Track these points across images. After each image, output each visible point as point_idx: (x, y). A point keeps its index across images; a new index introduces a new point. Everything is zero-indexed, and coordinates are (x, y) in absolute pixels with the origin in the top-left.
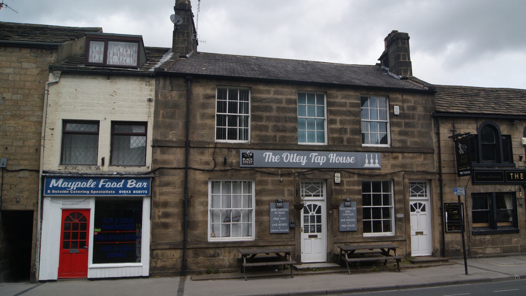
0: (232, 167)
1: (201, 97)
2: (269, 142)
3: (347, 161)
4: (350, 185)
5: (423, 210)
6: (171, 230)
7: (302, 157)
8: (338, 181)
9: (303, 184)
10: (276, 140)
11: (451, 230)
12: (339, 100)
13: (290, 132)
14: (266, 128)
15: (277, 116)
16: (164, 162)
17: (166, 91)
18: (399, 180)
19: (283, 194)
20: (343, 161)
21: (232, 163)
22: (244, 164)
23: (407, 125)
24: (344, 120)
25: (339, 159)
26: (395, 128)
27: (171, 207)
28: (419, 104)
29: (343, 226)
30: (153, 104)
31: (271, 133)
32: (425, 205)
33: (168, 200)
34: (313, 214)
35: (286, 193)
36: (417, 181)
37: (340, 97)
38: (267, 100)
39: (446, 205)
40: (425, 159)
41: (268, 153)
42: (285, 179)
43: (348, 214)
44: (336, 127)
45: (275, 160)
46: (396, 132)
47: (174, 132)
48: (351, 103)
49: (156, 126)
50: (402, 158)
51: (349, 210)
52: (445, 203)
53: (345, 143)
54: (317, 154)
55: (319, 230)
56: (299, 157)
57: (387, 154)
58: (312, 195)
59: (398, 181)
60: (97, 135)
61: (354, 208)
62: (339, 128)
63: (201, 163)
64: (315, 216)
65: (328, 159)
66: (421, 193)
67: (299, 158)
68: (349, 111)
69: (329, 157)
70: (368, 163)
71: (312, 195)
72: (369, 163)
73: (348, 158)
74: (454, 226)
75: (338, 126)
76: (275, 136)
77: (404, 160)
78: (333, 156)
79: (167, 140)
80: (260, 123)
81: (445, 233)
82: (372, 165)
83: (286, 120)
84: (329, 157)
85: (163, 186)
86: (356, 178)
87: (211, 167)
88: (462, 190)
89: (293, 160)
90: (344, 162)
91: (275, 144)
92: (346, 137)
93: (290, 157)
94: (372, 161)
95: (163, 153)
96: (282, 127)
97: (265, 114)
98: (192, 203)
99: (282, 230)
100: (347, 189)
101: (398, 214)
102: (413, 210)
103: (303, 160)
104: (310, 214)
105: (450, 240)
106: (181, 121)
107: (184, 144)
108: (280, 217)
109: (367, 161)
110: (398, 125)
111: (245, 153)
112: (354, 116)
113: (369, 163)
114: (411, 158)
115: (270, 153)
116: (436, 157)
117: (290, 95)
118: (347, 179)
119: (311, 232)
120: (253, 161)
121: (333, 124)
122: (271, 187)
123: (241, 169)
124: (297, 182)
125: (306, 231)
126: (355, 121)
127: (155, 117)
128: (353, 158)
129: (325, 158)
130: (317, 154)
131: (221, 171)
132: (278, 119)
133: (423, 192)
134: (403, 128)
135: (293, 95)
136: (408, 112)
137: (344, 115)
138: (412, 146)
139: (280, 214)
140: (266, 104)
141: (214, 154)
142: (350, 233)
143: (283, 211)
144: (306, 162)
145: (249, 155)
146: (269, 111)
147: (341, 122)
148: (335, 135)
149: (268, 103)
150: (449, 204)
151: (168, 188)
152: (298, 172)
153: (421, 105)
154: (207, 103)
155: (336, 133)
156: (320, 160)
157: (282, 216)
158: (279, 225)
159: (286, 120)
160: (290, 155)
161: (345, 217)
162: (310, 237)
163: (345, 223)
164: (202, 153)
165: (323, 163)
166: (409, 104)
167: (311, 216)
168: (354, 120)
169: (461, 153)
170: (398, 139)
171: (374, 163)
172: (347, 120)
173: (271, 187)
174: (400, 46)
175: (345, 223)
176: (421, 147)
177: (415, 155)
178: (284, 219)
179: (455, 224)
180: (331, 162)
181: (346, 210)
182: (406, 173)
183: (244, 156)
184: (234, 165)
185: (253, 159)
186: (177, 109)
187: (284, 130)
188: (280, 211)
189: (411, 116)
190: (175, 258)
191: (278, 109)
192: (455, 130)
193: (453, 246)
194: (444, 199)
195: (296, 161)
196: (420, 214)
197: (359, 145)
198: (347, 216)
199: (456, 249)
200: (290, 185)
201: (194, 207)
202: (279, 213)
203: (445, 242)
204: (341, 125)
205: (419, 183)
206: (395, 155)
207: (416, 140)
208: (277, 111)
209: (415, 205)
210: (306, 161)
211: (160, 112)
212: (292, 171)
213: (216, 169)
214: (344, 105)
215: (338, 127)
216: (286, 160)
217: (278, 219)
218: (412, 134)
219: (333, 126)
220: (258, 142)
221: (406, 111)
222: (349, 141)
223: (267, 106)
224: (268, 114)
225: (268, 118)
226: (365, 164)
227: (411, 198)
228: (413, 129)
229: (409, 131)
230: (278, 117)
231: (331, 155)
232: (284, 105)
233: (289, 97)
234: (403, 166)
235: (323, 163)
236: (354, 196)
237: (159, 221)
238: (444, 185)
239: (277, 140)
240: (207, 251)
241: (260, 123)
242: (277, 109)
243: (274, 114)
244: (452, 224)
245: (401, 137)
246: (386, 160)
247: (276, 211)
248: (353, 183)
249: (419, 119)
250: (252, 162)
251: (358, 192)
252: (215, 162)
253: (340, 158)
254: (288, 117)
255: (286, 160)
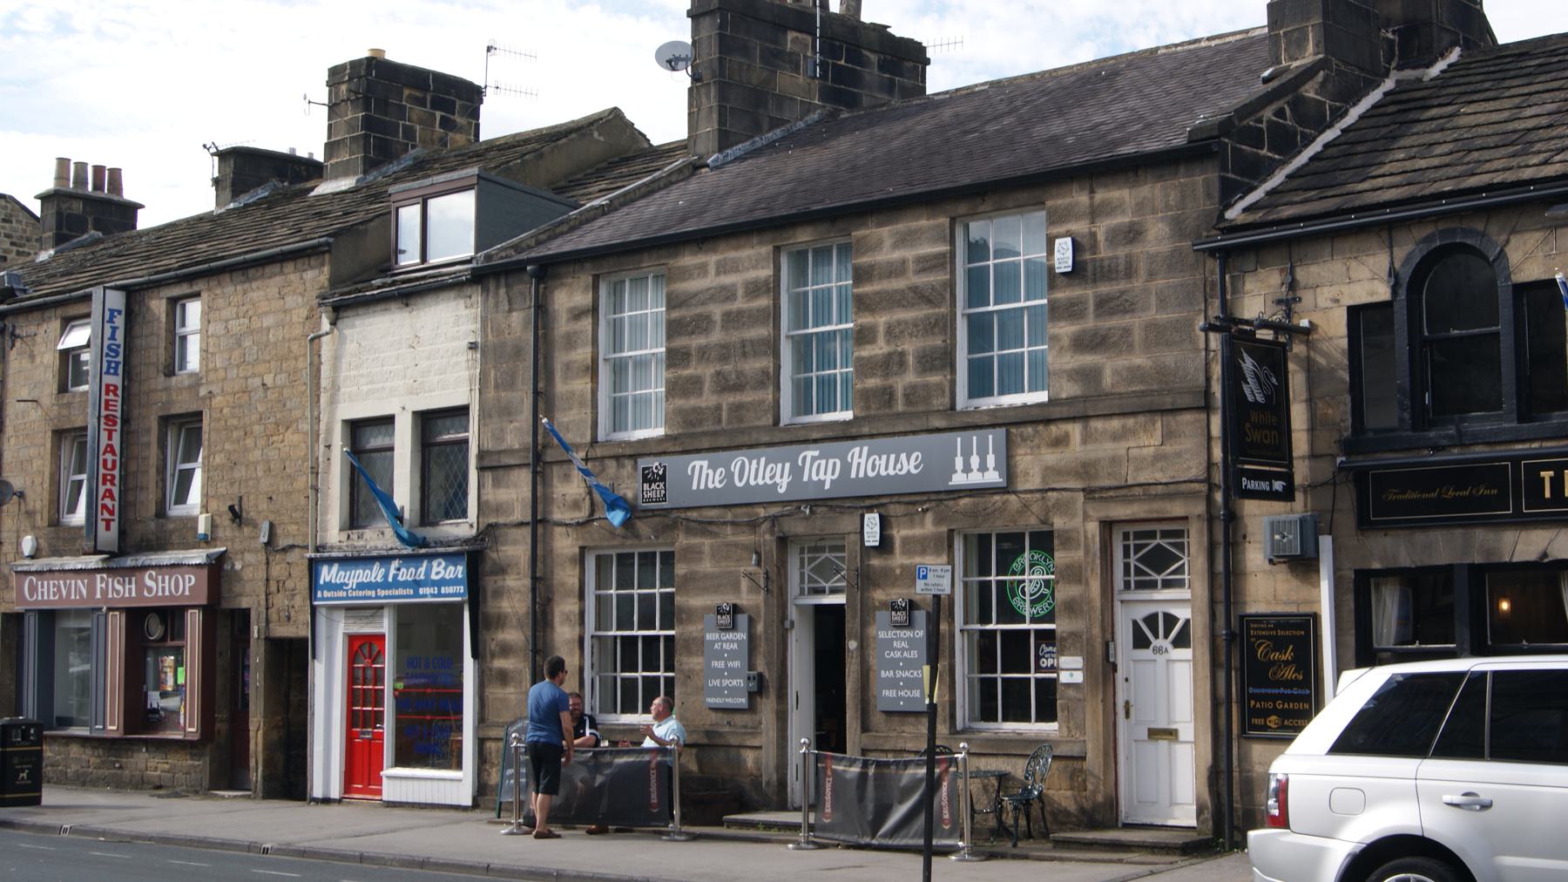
2: (705, 428)
3: (900, 470)
5: (1182, 641)
10: (720, 421)
12: (887, 255)
13: (754, 388)
17: (500, 316)
19: (736, 588)
20: (886, 469)
23: (1105, 306)
25: (877, 463)
26: (1063, 324)
28: (1154, 212)
29: (886, 693)
31: (707, 399)
35: (744, 583)
37: (888, 243)
40: (1168, 436)
41: (698, 463)
44: (873, 353)
46: (1066, 342)
48: (920, 260)
50: (1082, 439)
53: (900, 406)
54: (816, 453)
56: (772, 469)
59: (1067, 531)
62: (883, 354)
65: (846, 467)
68: (914, 289)
72: (967, 469)
73: (903, 456)
74: (1275, 711)
75: (880, 348)
76: (718, 408)
77: (1089, 447)
78: (860, 457)
82: (976, 478)
83: (747, 349)
86: (928, 527)
90: (891, 472)
91: (715, 434)
94: (975, 461)
95: (497, 484)
97: (696, 342)
99: (729, 700)
100: (903, 567)
103: (782, 477)
108: (726, 660)
111: (648, 468)
113: (967, 469)
114: (1116, 437)
117: (755, 267)
121: (868, 343)
124: (767, 548)
126: (930, 323)
130: (816, 453)
132: (725, 353)
134: (1090, 323)
135: (763, 268)
138: (1122, 390)
139: (726, 651)
140: (699, 310)
142: (911, 719)
143: (732, 641)
148: (873, 382)
149: (702, 304)
153: (1160, 215)
155: (873, 375)
156: (825, 474)
157: (733, 655)
158: (726, 682)
160: (750, 464)
163: (893, 683)
168: (927, 317)
171: (983, 468)
172: (906, 323)
175: (893, 683)
176: (1155, 387)
177: (1131, 421)
178: (736, 664)
180: (853, 475)
181: (897, 640)
183: (649, 477)
185: (665, 485)
187: (738, 387)
188: (727, 641)
189: (1121, 268)
196: (1165, 656)
198: (899, 660)
204: (888, 342)
206: (1054, 429)
207: (1139, 360)
208: (723, 327)
211: (489, 375)
212: (757, 514)
215: (880, 352)
219: (867, 352)
220: (680, 431)
221: (1104, 252)
222: (911, 394)
223: (699, 315)
225: (703, 353)
229: (1110, 329)
232: (740, 304)
233: (752, 275)
234: (1086, 469)
243: (716, 336)
244: (1270, 705)
245: (1081, 358)
249: (1152, 275)
250: (663, 492)
253: (880, 459)
254: (751, 341)
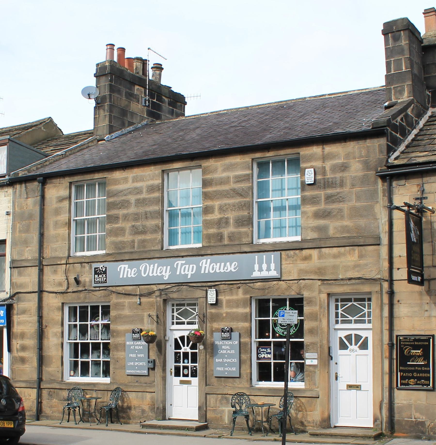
0: (85, 287)
1: (55, 201)
2: (126, 251)
3: (227, 270)
4: (232, 307)
5: (364, 346)
6: (27, 366)
7: (165, 267)
8: (211, 301)
9: (174, 306)
10: (134, 247)
11: (408, 384)
12: (219, 175)
13: (151, 233)
14: (122, 231)
15: (135, 212)
16: (21, 286)
17: (22, 200)
18: (310, 296)
19: (142, 321)
20: (220, 269)
21: (85, 282)
22: (96, 283)
23: (329, 199)
24: (226, 205)
25: (215, 266)
26: (308, 206)
27: (27, 338)
28: (354, 158)
29: (219, 369)
30: (11, 217)
31: (127, 238)
32: (367, 338)
33: (25, 330)
34: (186, 349)
35: (146, 319)
36: (353, 297)
37: (220, 169)
38: (124, 192)
39: (400, 340)
40: (361, 256)
41: (123, 266)
42: (145, 300)
43: (227, 352)
44: (212, 218)
45: (131, 275)
46: (310, 214)
47: (30, 249)
48: (236, 177)
49: (14, 244)
50: (318, 257)
51: (228, 345)
52: (397, 336)
53: (226, 242)
54: (184, 262)
55: (194, 374)
56: (161, 269)
57: (292, 252)
58: (186, 323)
59: (310, 298)
60: (4, 257)
61: (235, 343)
62: (217, 219)
63: (54, 284)
64: (188, 353)
65: (199, 268)
66: (360, 317)
67: (160, 270)
68: (234, 190)
69: (201, 265)
70: (258, 271)
71: (186, 323)
72: (261, 270)
73: (228, 264)
74: (413, 377)
75: (216, 216)
76: (133, 241)
77: (321, 261)
78: (206, 264)
79: (24, 259)
80: (116, 226)
81: (395, 390)
82: (265, 274)
83: (147, 216)
84: (201, 265)
85: (20, 315)
86: (240, 295)
87: (63, 288)
88: (293, 314)
89: (153, 273)
90: (222, 270)
91: (132, 253)
92: (226, 232)
93: (150, 269)
94: (264, 266)
95: (20, 274)
96: (141, 228)
97: (122, 212)
98: (46, 334)
99: (138, 371)
100: (227, 313)
101: (307, 353)
102: (343, 346)
103: (166, 272)
104: (182, 351)
105: (405, 402)
106: (35, 234)
107: (37, 262)
108: (136, 353)
109: (256, 267)
110: (314, 201)
111: (98, 268)
112: (241, 195)
113: (261, 270)
114: (335, 256)
115: (125, 266)
116: (384, 250)
117: (152, 179)
118: (228, 298)
119: (183, 376)
120: (106, 278)
121: (210, 213)
122: (128, 312)
123: (94, 289)
124: (158, 304)
125: (177, 374)
126: (241, 205)
127: (12, 233)
128: (135, 270)
129: (195, 266)
130: (184, 262)
131: (74, 292)
132: (136, 217)
133: (364, 316)
134: (322, 206)
135: (156, 180)
136: (332, 176)
137: (225, 198)
138: (338, 236)
139: (137, 350)
140: (124, 198)
141: (66, 272)
142: (231, 380)
143: (140, 345)
144: (169, 275)
145: (102, 270)
146: (126, 207)
147: (221, 209)
148: (212, 231)
149: (125, 196)
150: (406, 337)
151: (24, 316)
152: (160, 290)
153: (357, 160)
154: (60, 208)
155: (213, 228)
156: (188, 271)
157: (140, 351)
158: (136, 364)
159: (146, 217)
160: (150, 267)
161: (223, 356)
162: (182, 382)
163: (222, 364)
164: (55, 272)
165: (191, 274)
166: (335, 162)
167: (183, 353)
168: (240, 202)
169: (413, 240)
170: (312, 225)
171: (269, 269)
172: (229, 205)
173: (128, 312)
174: (391, 46)
175: (222, 364)
176: (355, 235)
177: (342, 249)
178: (142, 355)
179: (415, 375)
180: (202, 272)
181: (224, 345)
182: (325, 282)
183: (97, 272)
184: (87, 284)
185: (106, 276)
186: (32, 220)
187: (144, 232)
188: (137, 345)
189: (338, 182)
190: (32, 399)
191: (139, 202)
192: (425, 196)
193: (411, 415)
194: (395, 328)
195: (156, 275)
196: (356, 353)
197: (247, 243)
198: (225, 354)
199: (416, 421)
200: (150, 309)
201: (48, 339)
202: (136, 347)
203: (396, 405)
204: (220, 213)
205: (356, 300)
206: (305, 252)
207: (347, 223)
208: (136, 206)
209: (348, 337)
210: (169, 272)
211: (17, 226)
212: (153, 289)
213: (69, 291)
214: (222, 182)
215: (216, 217)
216: (145, 274)
217: (134, 356)
218: (340, 214)
219: (209, 217)
220: (113, 252)
221: (329, 175)
222: (231, 237)
223: (123, 200)
224: (125, 211)
225: (126, 217)
226: (253, 273)
227: (175, 327)
228: (341, 205)
229: (332, 209)
230: (137, 214)
231: (203, 262)
232: (144, 195)
233: (151, 182)
234: (320, 271)
235: (191, 274)
236: (238, 322)
237: (17, 355)
238: (398, 301)
239: (136, 246)
240: (60, 392)
241: (116, 226)
242: (135, 203)
243: (132, 210)
244: (410, 375)
245: (318, 221)
246: (290, 264)
247: (132, 345)
248: (237, 304)
249: (353, 186)
250: (105, 279)
251: (247, 318)
252: (68, 282)
253: (216, 265)
254: (150, 212)
255: (145, 274)
